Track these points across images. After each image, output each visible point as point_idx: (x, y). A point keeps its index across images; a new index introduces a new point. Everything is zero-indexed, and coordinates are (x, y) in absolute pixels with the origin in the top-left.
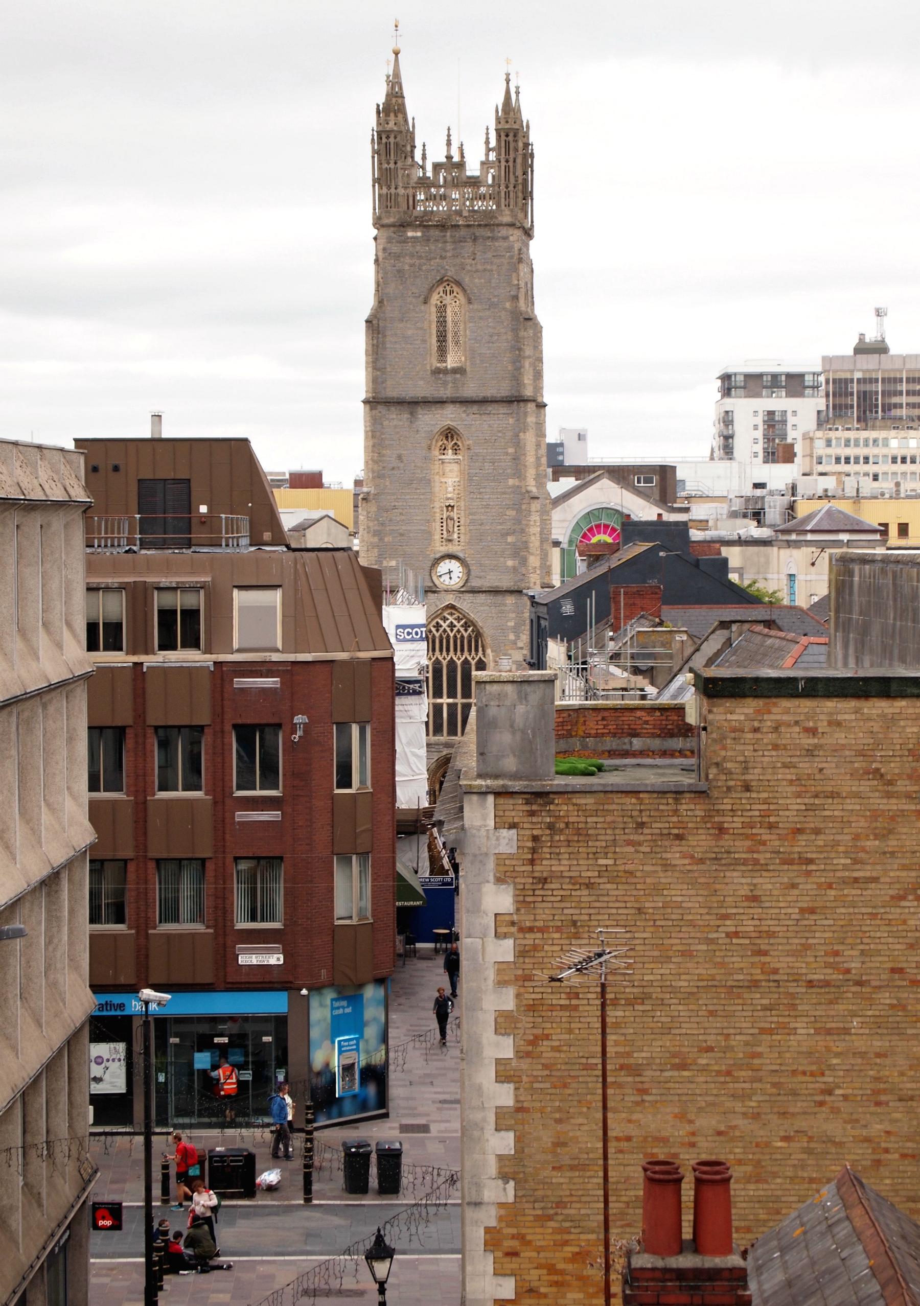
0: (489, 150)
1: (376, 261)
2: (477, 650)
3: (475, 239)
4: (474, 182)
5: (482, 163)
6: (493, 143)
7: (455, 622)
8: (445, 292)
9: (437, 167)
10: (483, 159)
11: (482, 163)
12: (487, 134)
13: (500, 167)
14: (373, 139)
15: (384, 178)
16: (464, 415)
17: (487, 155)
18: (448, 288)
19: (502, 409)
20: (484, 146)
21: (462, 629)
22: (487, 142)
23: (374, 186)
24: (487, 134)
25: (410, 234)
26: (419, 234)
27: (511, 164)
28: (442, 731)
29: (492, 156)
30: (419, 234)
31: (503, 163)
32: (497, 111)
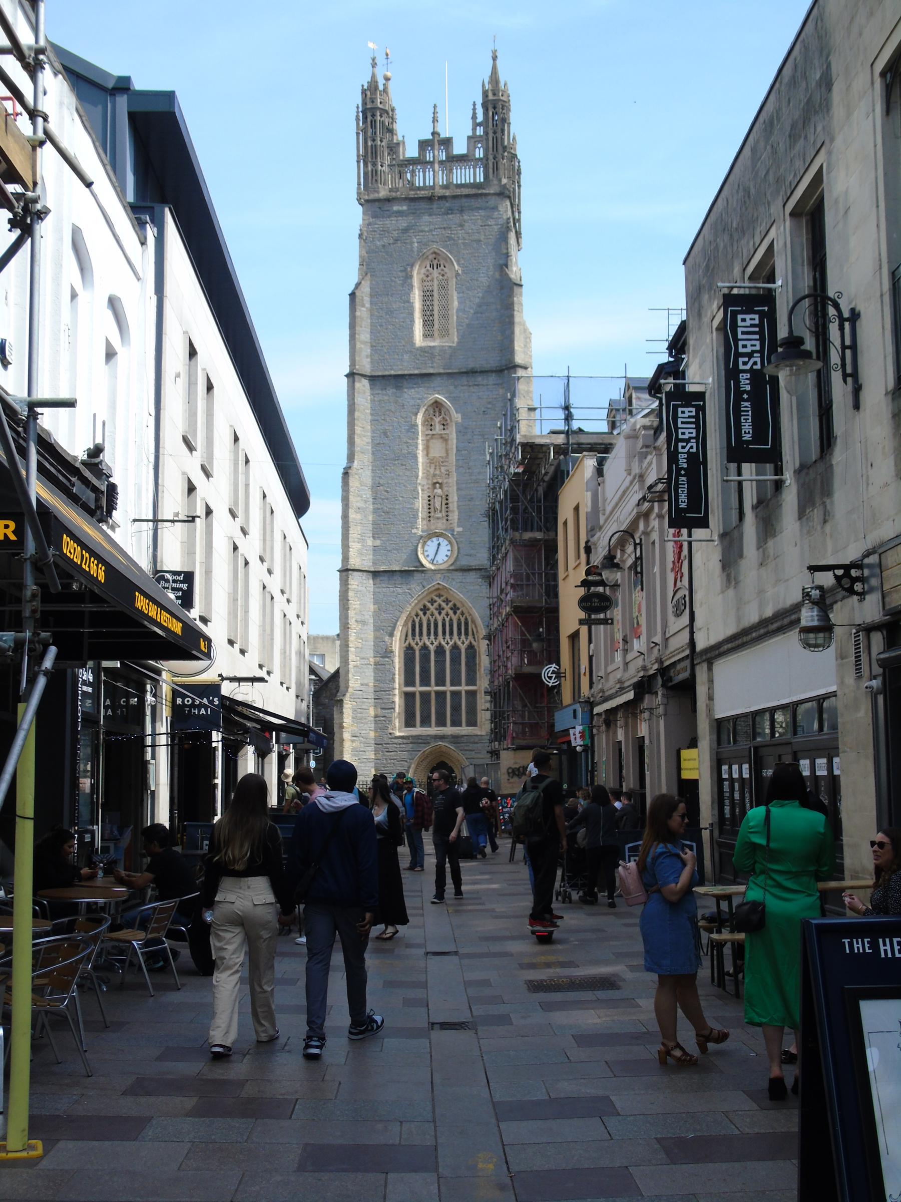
0: (476, 125)
1: (360, 236)
2: (467, 634)
3: (462, 211)
4: (462, 159)
5: (469, 138)
6: (480, 118)
7: (444, 605)
8: (432, 266)
9: (423, 145)
10: (470, 134)
11: (469, 138)
12: (474, 109)
13: (487, 140)
14: (357, 117)
15: (369, 155)
16: (452, 388)
17: (474, 130)
18: (435, 262)
19: (492, 379)
20: (470, 122)
21: (451, 612)
22: (474, 117)
23: (358, 162)
24: (474, 109)
25: (395, 208)
26: (405, 208)
27: (499, 135)
28: (430, 722)
29: (480, 131)
30: (405, 208)
31: (491, 135)
32: (483, 85)
